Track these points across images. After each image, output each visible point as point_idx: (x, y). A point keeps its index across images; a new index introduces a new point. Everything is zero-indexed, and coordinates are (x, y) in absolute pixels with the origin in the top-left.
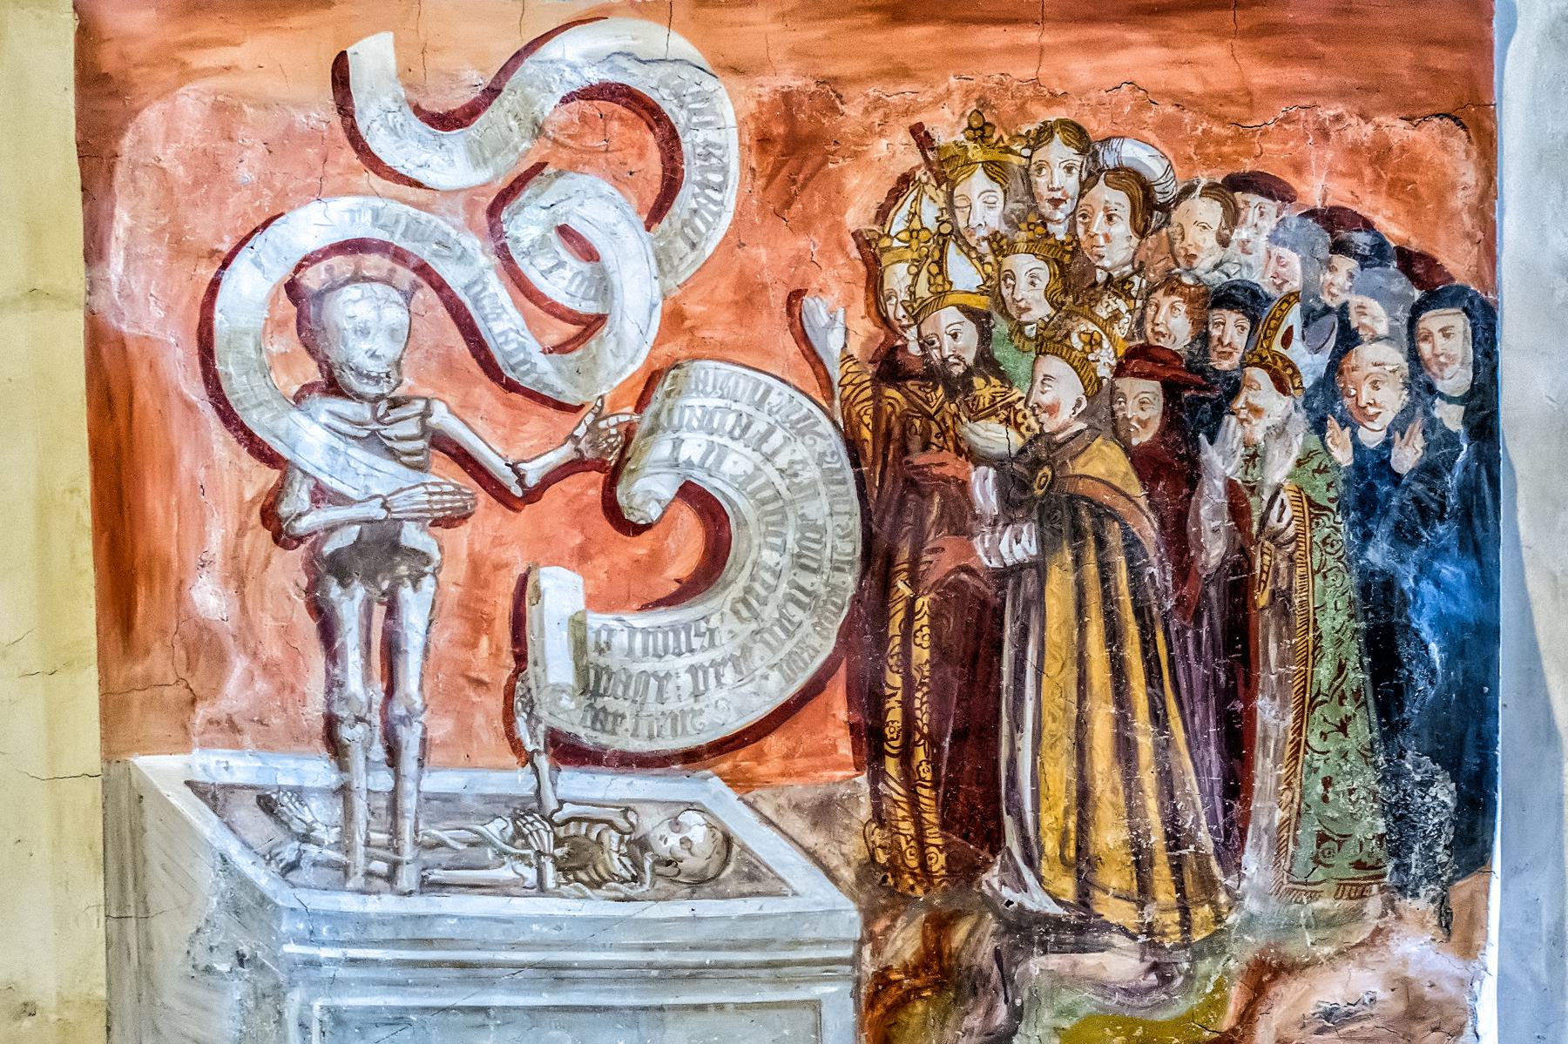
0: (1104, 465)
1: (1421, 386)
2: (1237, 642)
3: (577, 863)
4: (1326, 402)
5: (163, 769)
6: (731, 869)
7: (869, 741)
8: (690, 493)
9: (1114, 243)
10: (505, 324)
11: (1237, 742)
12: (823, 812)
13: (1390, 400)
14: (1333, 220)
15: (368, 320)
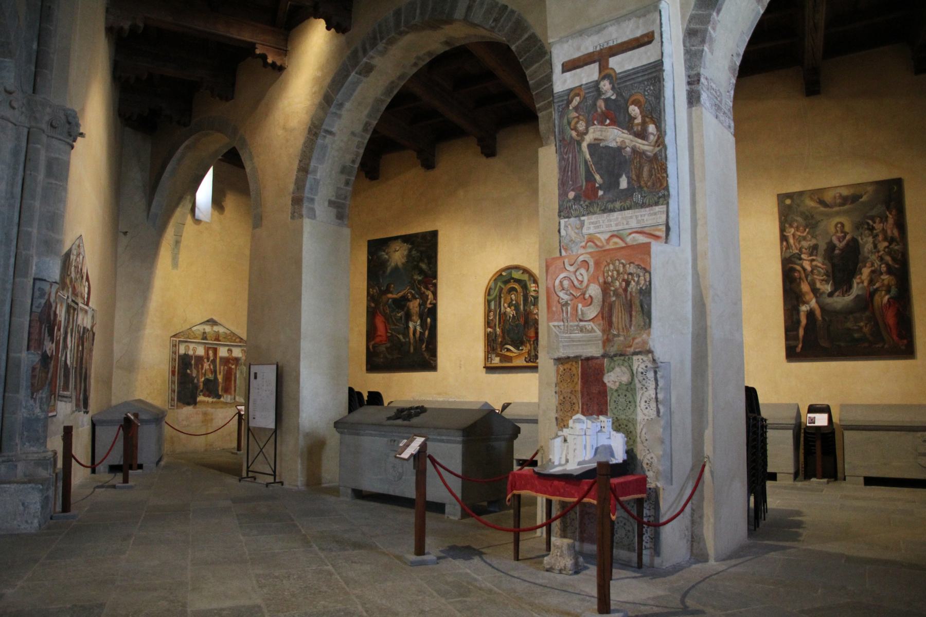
0: (621, 291)
1: (645, 280)
2: (631, 307)
3: (581, 331)
4: (638, 283)
5: (551, 324)
6: (592, 331)
7: (603, 318)
8: (590, 296)
9: (621, 270)
10: (576, 283)
11: (631, 316)
12: (599, 325)
13: (642, 282)
14: (638, 265)
15: (566, 283)
